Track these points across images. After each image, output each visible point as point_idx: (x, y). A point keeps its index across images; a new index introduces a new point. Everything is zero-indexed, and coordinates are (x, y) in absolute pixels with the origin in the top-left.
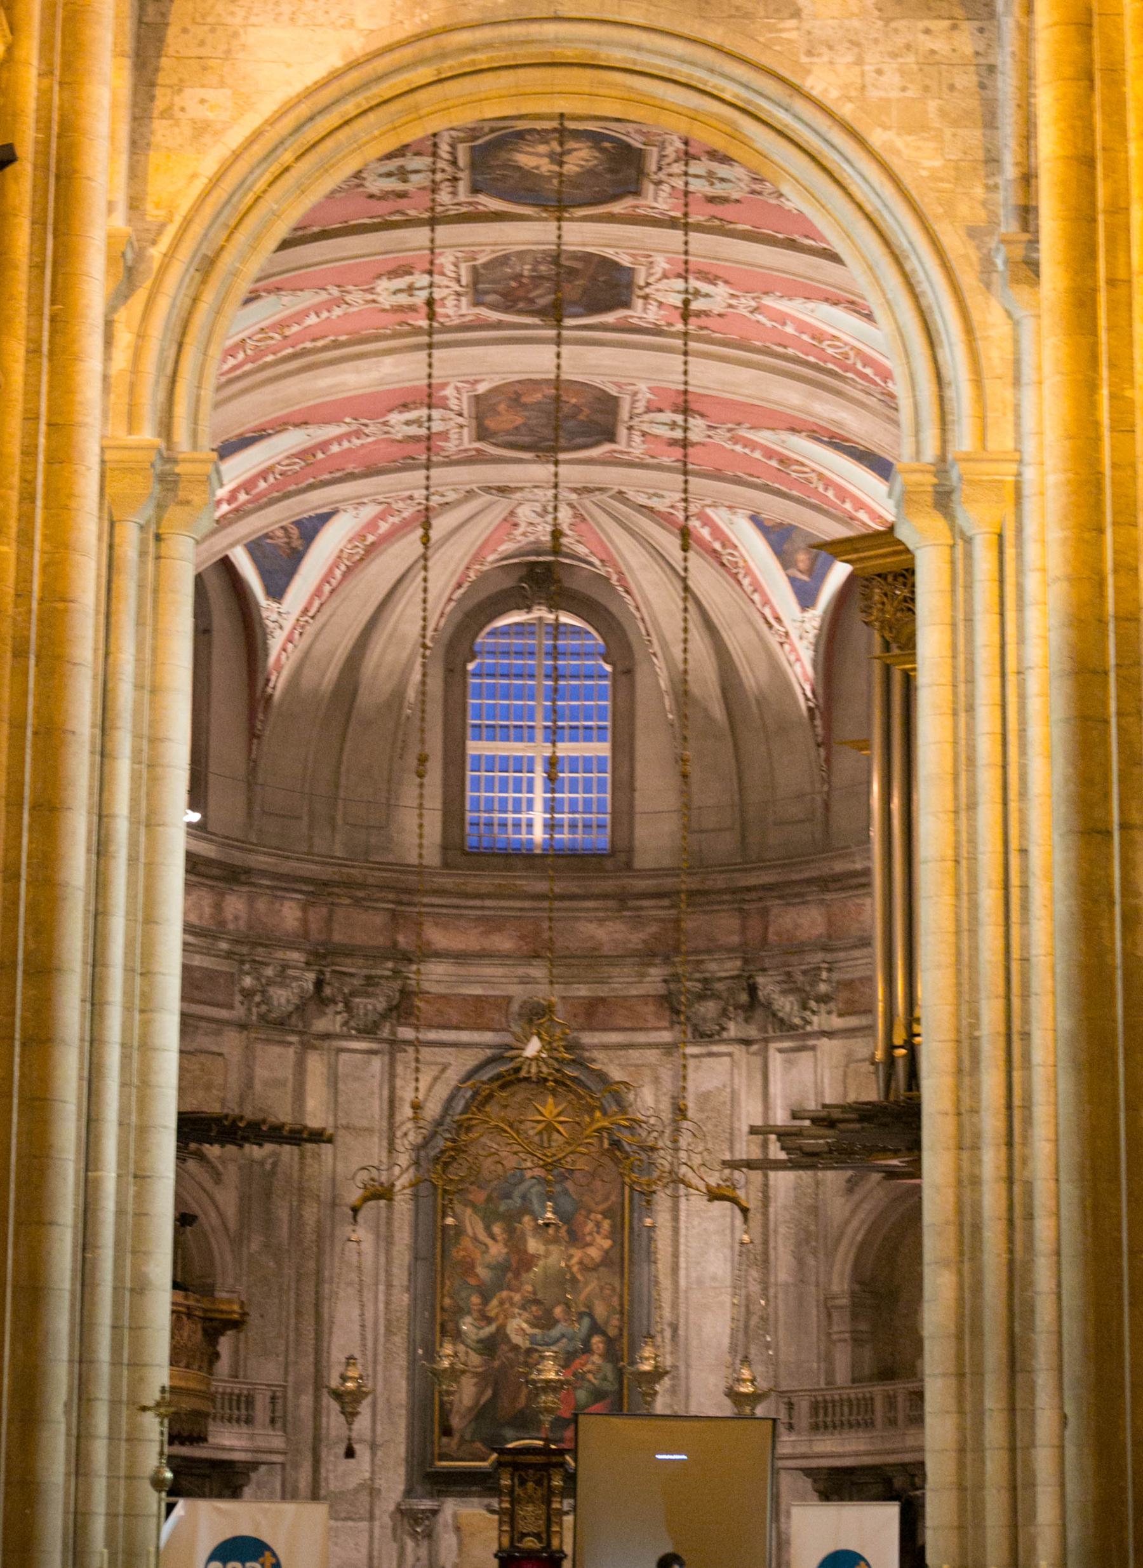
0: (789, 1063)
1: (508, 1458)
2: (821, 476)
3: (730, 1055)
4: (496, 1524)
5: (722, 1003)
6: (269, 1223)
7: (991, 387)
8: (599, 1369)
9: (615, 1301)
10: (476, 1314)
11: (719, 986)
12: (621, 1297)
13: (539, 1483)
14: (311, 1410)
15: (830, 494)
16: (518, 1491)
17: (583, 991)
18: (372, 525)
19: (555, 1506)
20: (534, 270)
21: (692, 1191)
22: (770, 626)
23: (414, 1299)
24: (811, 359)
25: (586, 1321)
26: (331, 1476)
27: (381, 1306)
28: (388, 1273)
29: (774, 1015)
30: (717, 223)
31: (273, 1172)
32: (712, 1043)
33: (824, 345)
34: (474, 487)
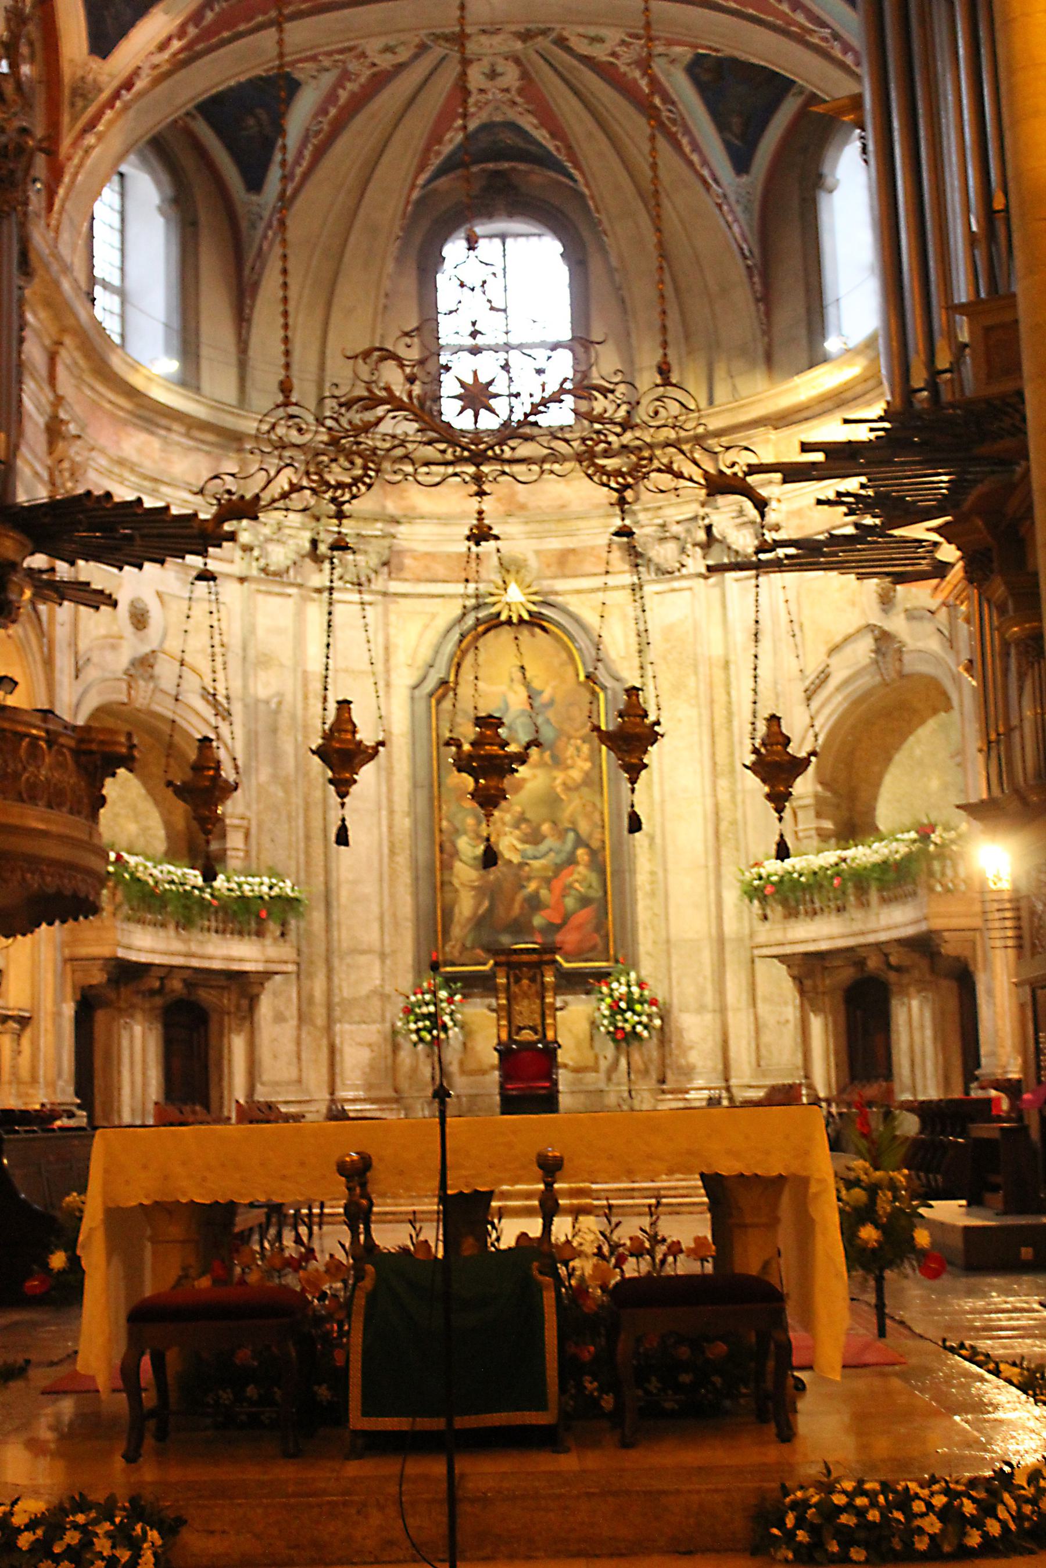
1: (502, 958)
3: (690, 589)
4: (495, 1022)
5: (681, 543)
6: (276, 758)
8: (585, 879)
9: (597, 817)
10: (472, 835)
12: (602, 814)
13: (532, 980)
14: (323, 925)
16: (515, 989)
17: (555, 544)
19: (549, 1000)
21: (683, 483)
23: (415, 822)
25: (571, 836)
26: (344, 984)
27: (385, 829)
28: (390, 801)
29: (729, 548)
31: (277, 712)
32: (672, 580)
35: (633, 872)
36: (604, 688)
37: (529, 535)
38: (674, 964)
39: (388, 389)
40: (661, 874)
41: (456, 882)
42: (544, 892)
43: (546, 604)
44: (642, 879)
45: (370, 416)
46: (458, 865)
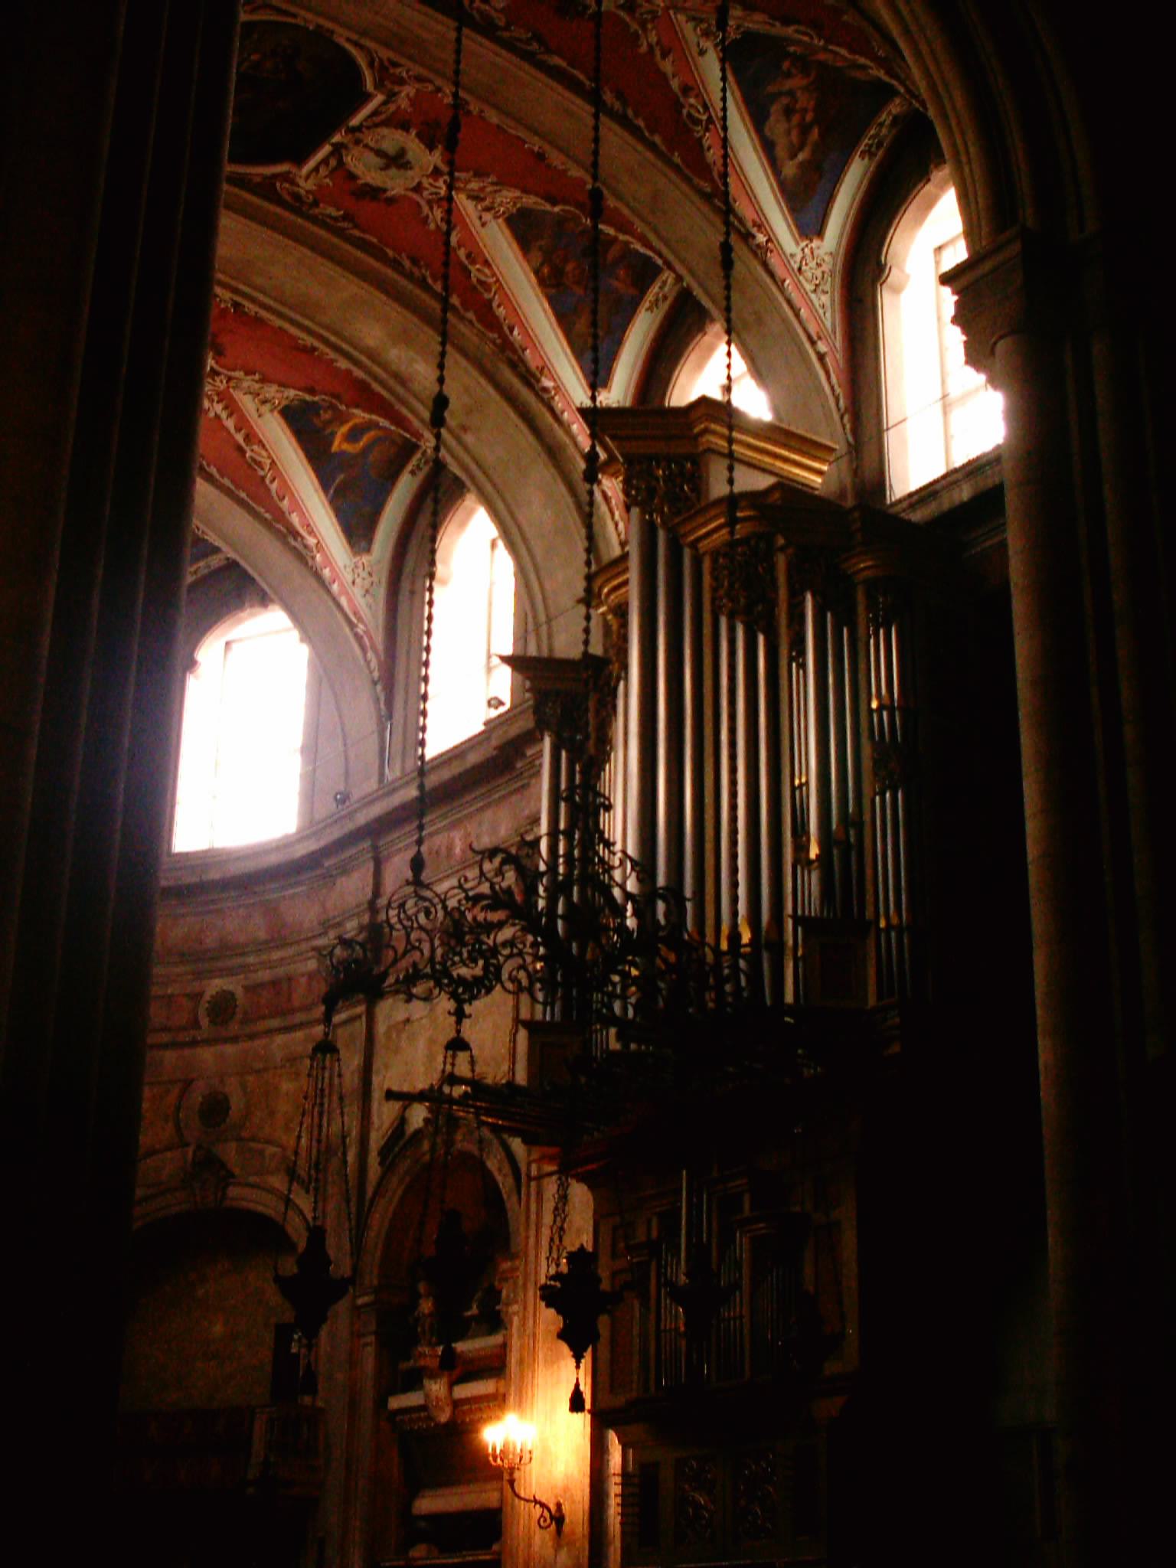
2: (273, 462)
15: (274, 487)
33: (470, 267)
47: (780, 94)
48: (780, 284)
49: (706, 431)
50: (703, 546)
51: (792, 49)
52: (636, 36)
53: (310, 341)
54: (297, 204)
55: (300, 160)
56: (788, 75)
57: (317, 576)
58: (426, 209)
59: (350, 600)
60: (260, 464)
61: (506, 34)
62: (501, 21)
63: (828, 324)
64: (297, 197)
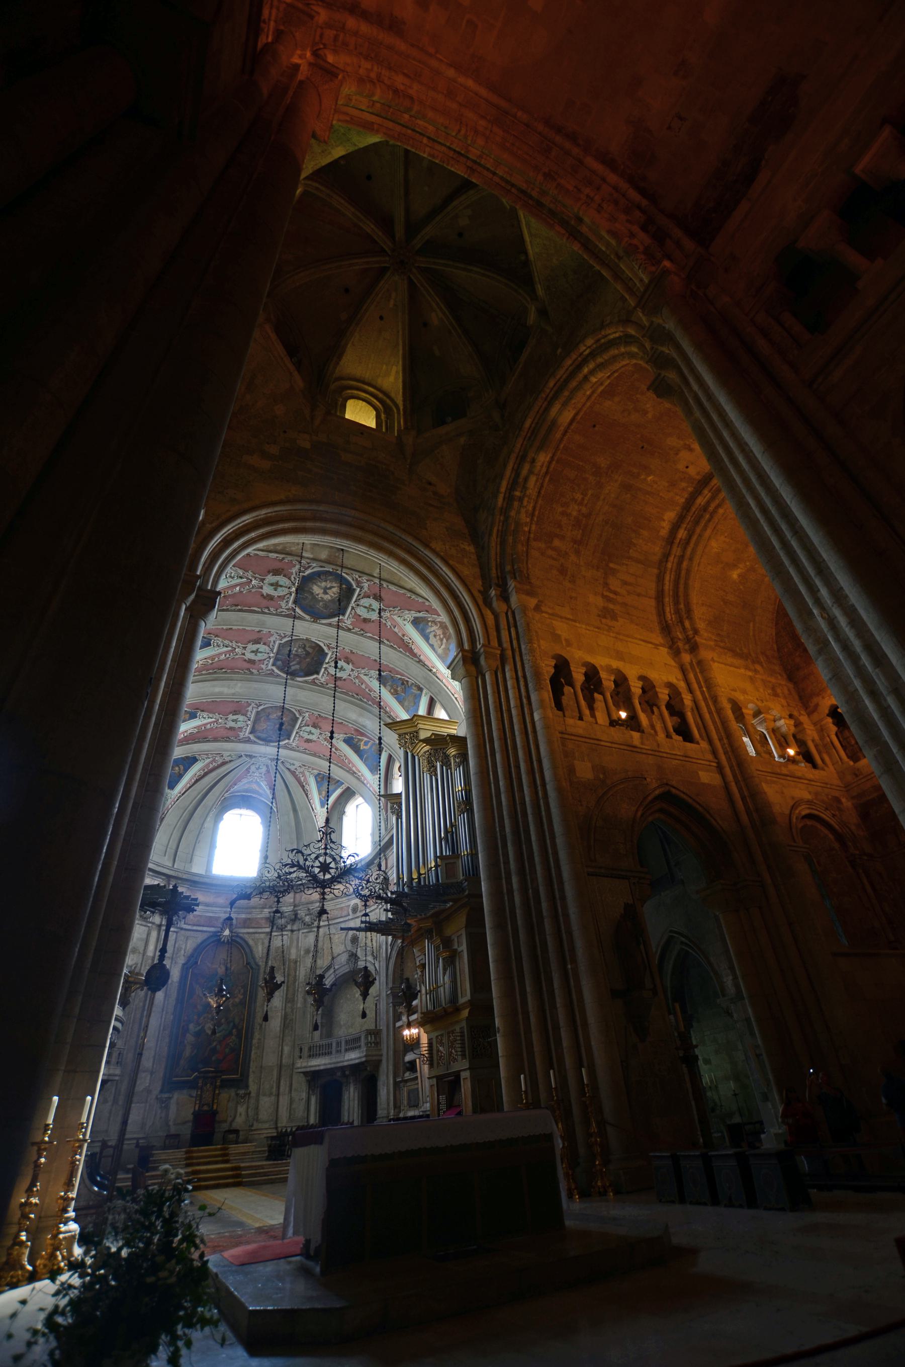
0: (306, 936)
3: (287, 935)
7: (490, 631)
11: (287, 914)
12: (244, 1015)
15: (346, 761)
17: (243, 916)
18: (208, 765)
20: (296, 651)
22: (313, 810)
24: (365, 700)
25: (232, 1024)
27: (163, 1019)
30: (362, 632)
34: (243, 753)
35: (252, 1038)
36: (252, 968)
37: (235, 912)
38: (262, 1076)
39: (298, 862)
40: (262, 1039)
41: (186, 1042)
42: (218, 1047)
43: (237, 936)
44: (255, 1041)
45: (292, 870)
46: (188, 1035)
47: (431, 632)
48: (442, 681)
49: (418, 723)
50: (420, 755)
51: (429, 619)
52: (385, 624)
53: (341, 721)
54: (322, 686)
55: (318, 673)
56: (432, 626)
57: (363, 783)
58: (354, 681)
59: (373, 788)
60: (342, 756)
61: (354, 630)
62: (351, 627)
63: (458, 689)
64: (322, 684)
